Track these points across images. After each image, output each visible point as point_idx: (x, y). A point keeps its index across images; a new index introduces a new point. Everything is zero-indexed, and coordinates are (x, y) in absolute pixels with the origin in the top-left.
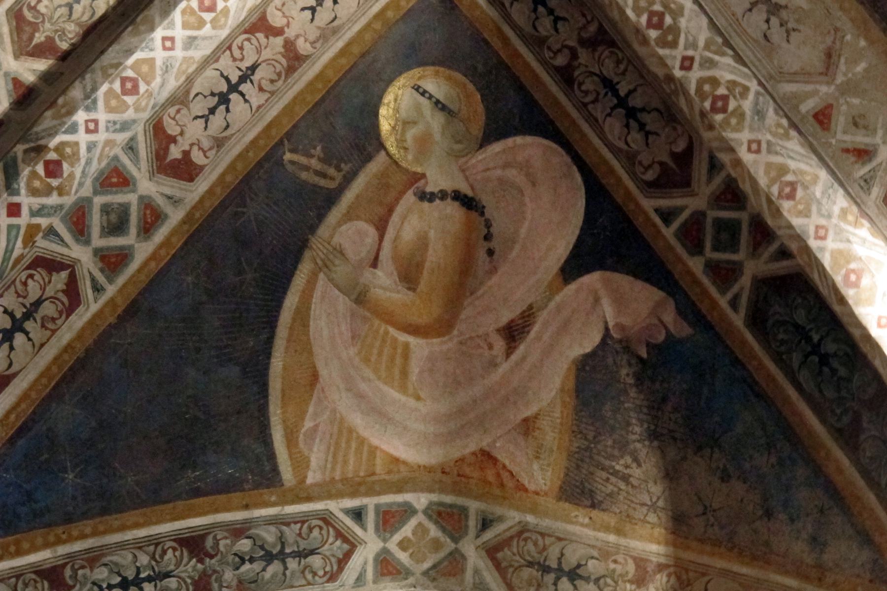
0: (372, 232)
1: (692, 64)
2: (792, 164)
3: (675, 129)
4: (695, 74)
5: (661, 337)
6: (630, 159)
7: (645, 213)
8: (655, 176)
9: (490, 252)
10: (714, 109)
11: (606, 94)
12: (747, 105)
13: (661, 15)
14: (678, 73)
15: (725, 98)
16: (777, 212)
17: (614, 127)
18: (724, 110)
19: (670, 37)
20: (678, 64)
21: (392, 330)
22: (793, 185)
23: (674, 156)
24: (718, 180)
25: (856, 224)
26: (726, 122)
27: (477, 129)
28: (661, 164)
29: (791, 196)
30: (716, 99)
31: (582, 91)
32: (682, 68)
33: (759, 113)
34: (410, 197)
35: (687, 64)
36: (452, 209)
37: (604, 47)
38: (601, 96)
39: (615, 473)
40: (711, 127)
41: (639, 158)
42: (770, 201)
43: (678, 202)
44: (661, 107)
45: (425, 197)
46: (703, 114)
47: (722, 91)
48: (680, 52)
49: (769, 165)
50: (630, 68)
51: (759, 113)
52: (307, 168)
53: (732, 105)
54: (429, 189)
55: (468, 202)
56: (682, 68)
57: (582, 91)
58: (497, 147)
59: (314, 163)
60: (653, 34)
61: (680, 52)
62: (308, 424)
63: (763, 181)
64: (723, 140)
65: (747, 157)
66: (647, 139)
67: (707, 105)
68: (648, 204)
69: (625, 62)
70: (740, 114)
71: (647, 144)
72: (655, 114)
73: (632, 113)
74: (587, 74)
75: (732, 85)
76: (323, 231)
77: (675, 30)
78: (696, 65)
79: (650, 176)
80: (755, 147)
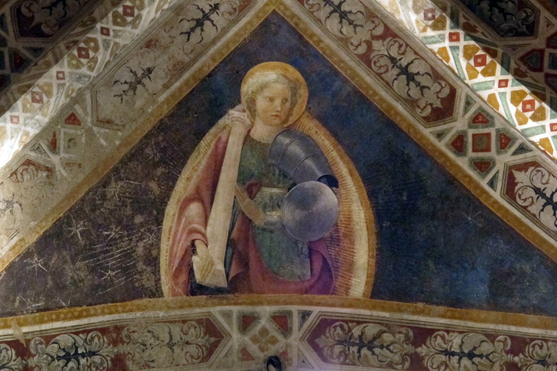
1: (105, 34)
2: (53, 100)
3: (55, 25)
4: (99, 37)
8: (24, 13)
10: (80, 50)
12: (84, 70)
13: (132, 15)
14: (98, 26)
15: (87, 56)
16: (23, 91)
18: (80, 56)
19: (119, 20)
20: (104, 26)
22: (40, 101)
23: (39, 26)
24: (28, 54)
25: (21, 142)
26: (73, 57)
28: (33, 17)
29: (34, 100)
30: (86, 50)
32: (102, 29)
33: (80, 78)
35: (105, 31)
40: (68, 48)
41: (34, 3)
42: (29, 86)
43: (10, 28)
44: (68, 16)
46: (76, 43)
47: (91, 54)
48: (112, 27)
49: (50, 85)
51: (80, 78)
53: (84, 61)
56: (102, 29)
60: (120, 10)
61: (112, 27)
63: (41, 81)
64: (62, 56)
65: (54, 70)
67: (82, 45)
70: (78, 67)
71: (43, 8)
72: (63, 13)
75: (94, 59)
77: (124, 23)
78: (104, 37)
79: (24, 10)
80: (60, 76)
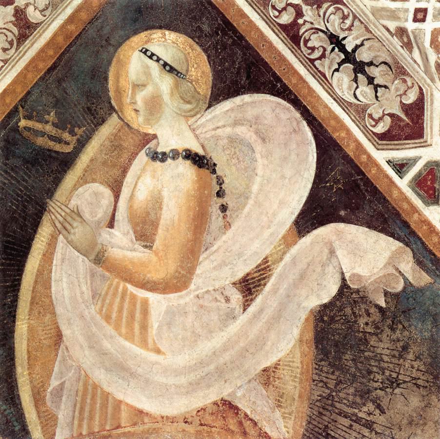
0: (107, 193)
1: (425, 16)
3: (405, 81)
5: (399, 287)
6: (359, 112)
7: (377, 165)
8: (386, 128)
9: (224, 208)
11: (333, 50)
17: (343, 81)
20: (411, 16)
21: (131, 288)
23: (406, 108)
27: (205, 88)
28: (391, 115)
31: (309, 48)
32: (415, 20)
34: (142, 158)
35: (420, 16)
36: (185, 168)
37: (329, 4)
38: (327, 53)
39: (358, 420)
41: (369, 111)
44: (389, 60)
45: (159, 157)
50: (356, 23)
52: (43, 134)
54: (159, 150)
55: (198, 160)
56: (415, 20)
57: (309, 48)
58: (226, 105)
59: (49, 128)
62: (54, 383)
66: (376, 92)
68: (381, 156)
69: (351, 18)
71: (377, 97)
72: (383, 68)
73: (360, 68)
74: (313, 31)
76: (61, 193)
78: (429, 17)
79: (380, 129)
